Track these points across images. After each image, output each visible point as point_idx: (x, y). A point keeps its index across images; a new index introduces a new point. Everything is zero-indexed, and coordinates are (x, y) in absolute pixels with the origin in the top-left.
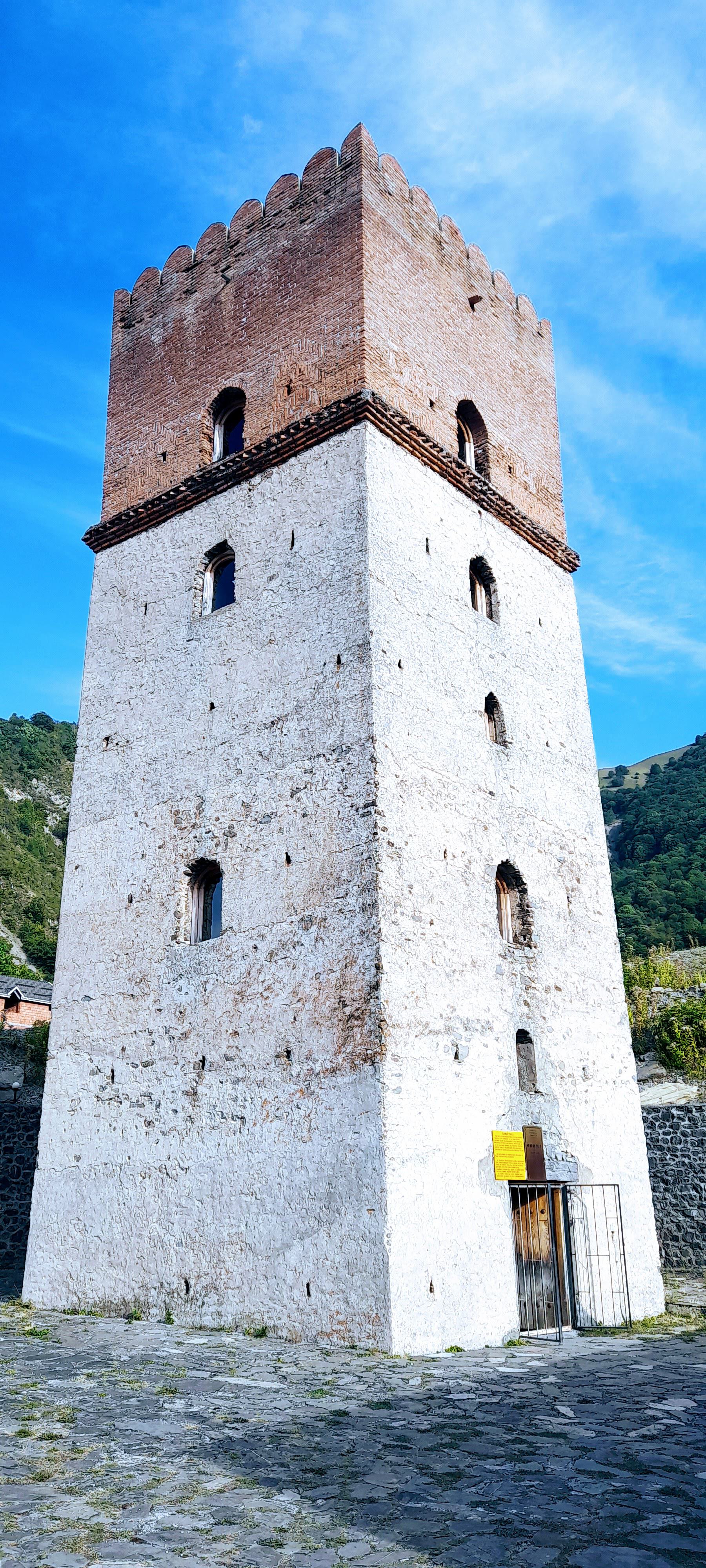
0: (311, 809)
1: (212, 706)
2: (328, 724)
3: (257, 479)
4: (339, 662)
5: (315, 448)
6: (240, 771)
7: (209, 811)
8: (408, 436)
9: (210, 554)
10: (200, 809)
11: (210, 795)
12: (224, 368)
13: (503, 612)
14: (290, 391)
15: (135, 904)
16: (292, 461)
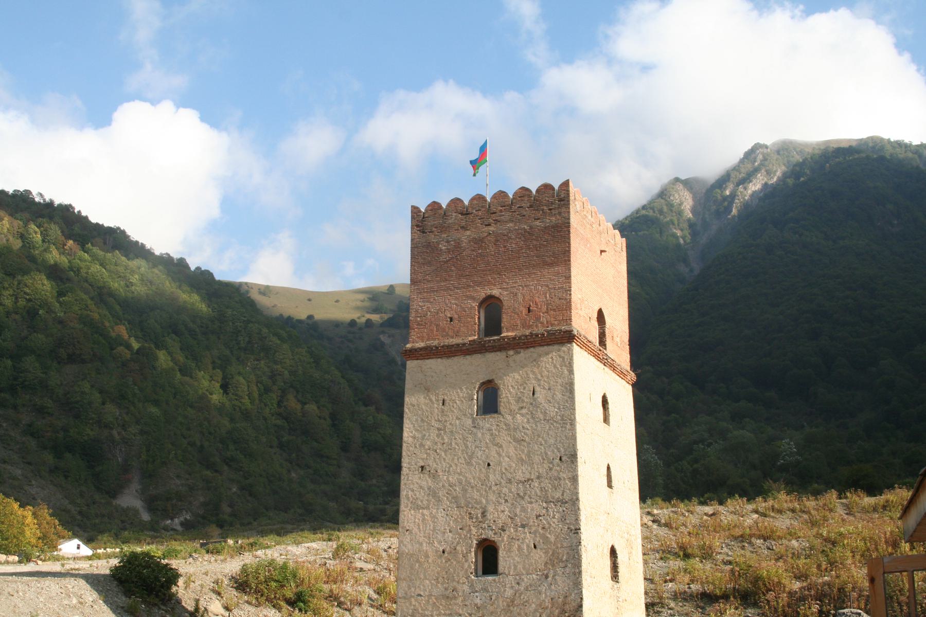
0: (547, 526)
1: (489, 465)
2: (555, 488)
3: (511, 352)
4: (560, 459)
5: (546, 347)
6: (506, 501)
7: (490, 517)
8: (586, 345)
9: (483, 384)
10: (484, 514)
11: (490, 508)
12: (489, 283)
13: (612, 419)
14: (529, 311)
15: (446, 554)
16: (532, 349)
